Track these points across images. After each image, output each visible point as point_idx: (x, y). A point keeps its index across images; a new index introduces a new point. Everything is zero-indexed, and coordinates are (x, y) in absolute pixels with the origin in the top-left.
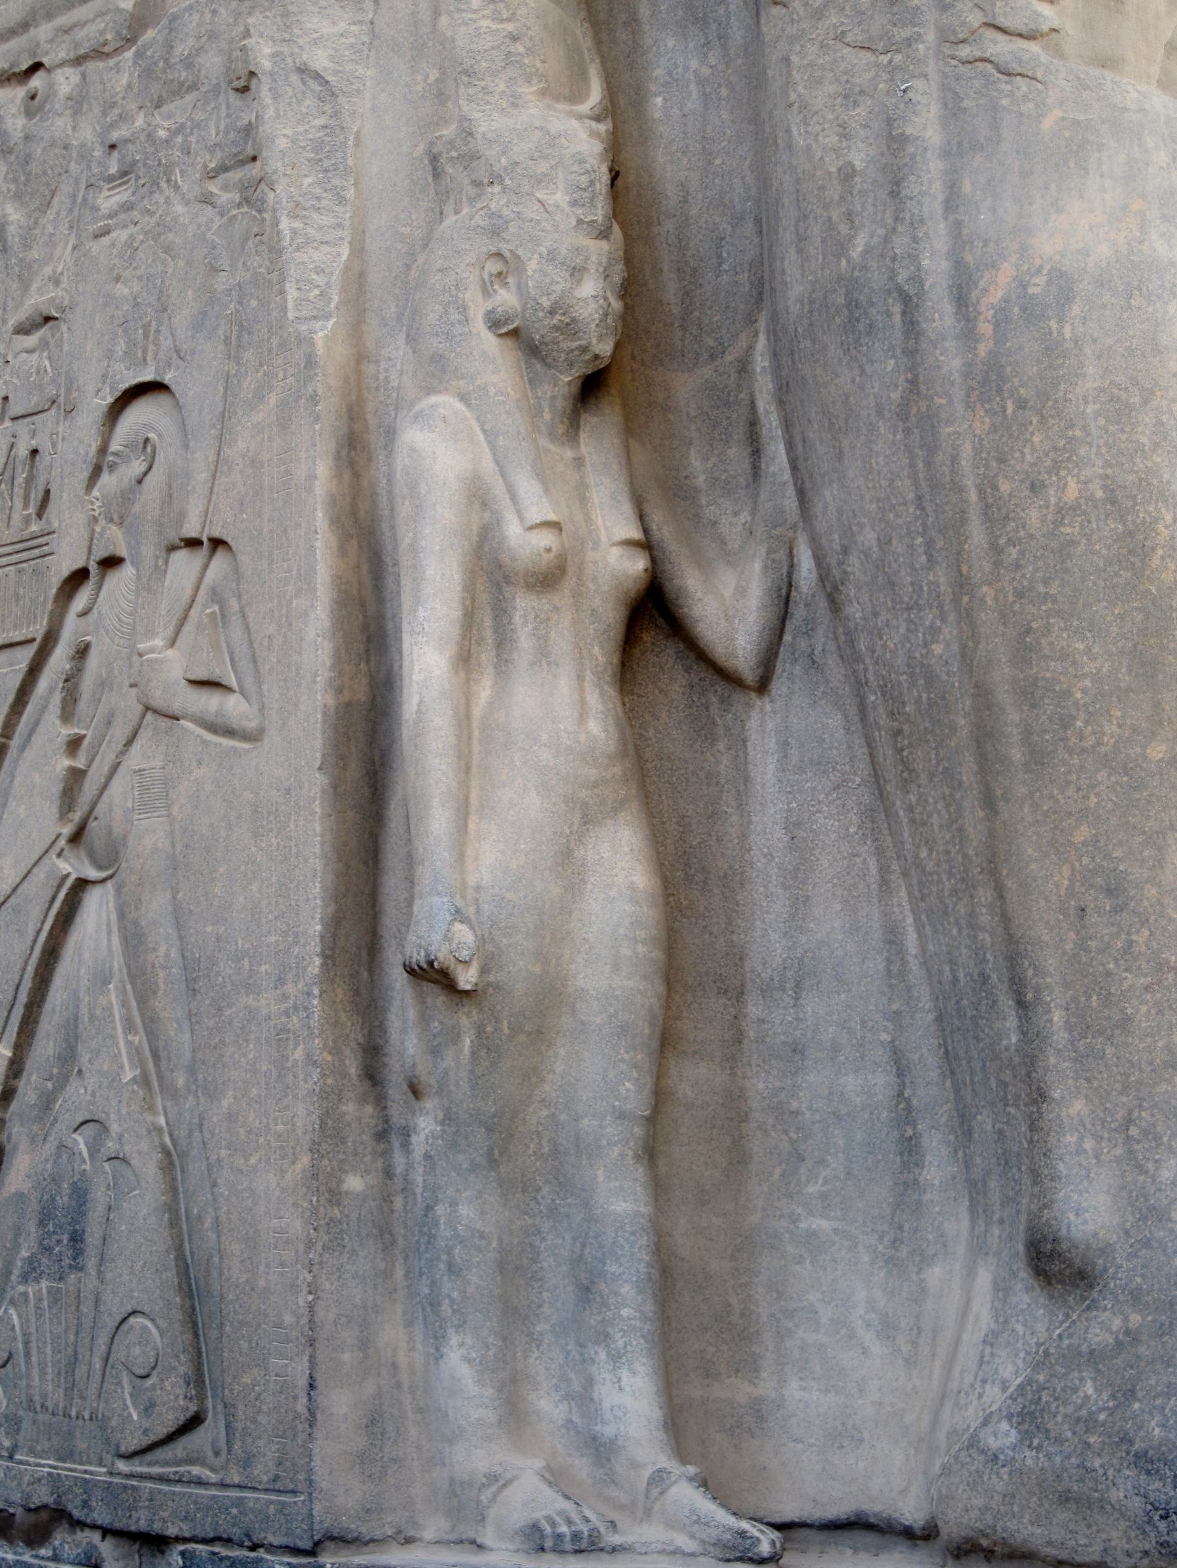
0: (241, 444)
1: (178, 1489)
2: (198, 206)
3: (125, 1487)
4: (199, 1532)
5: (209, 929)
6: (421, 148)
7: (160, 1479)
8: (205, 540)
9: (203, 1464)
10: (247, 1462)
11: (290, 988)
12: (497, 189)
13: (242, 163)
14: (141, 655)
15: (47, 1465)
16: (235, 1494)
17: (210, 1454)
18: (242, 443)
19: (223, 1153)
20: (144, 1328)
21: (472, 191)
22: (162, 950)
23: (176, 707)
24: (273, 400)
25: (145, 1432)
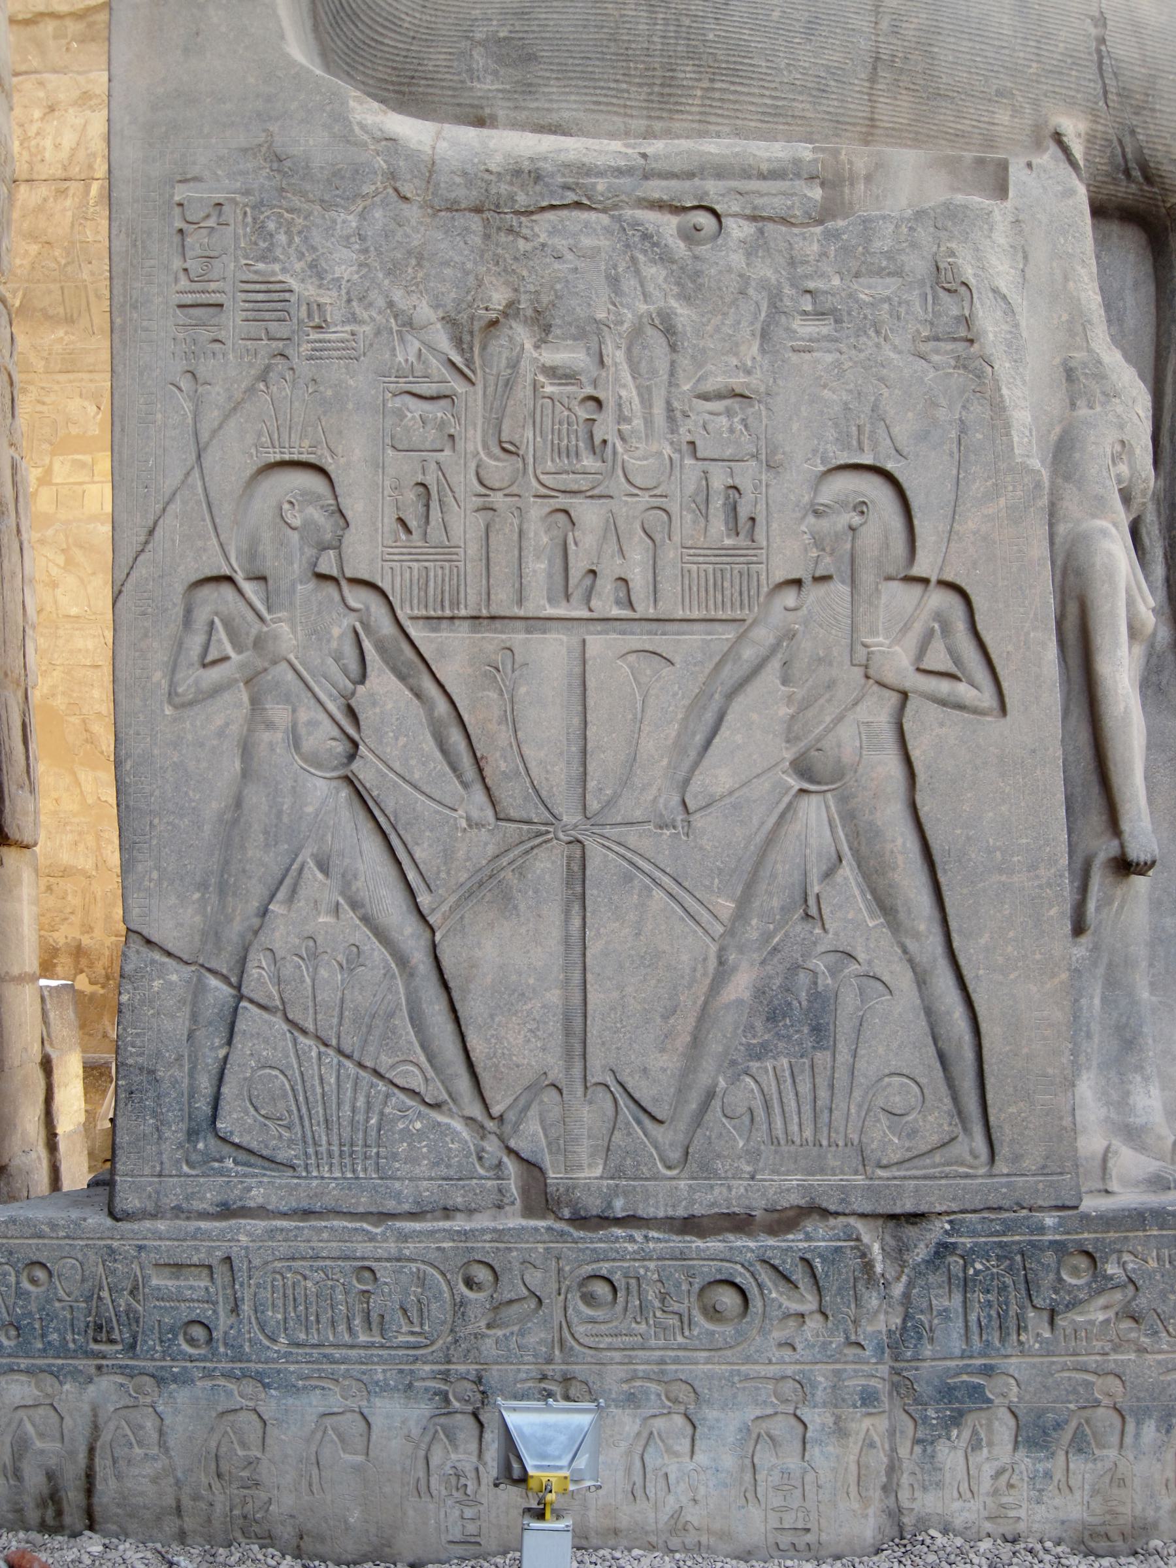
0: (971, 525)
1: (943, 1182)
2: (911, 358)
3: (888, 1186)
4: (968, 1206)
5: (958, 832)
6: (1058, 360)
7: (925, 1177)
8: (934, 579)
9: (962, 1164)
10: (1017, 1158)
11: (1042, 872)
12: (1117, 401)
13: (955, 340)
14: (865, 646)
15: (794, 1180)
16: (1004, 1180)
17: (969, 1158)
18: (971, 523)
19: (981, 972)
20: (902, 1085)
21: (1103, 398)
22: (899, 841)
23: (907, 685)
24: (1002, 501)
25: (909, 1149)
